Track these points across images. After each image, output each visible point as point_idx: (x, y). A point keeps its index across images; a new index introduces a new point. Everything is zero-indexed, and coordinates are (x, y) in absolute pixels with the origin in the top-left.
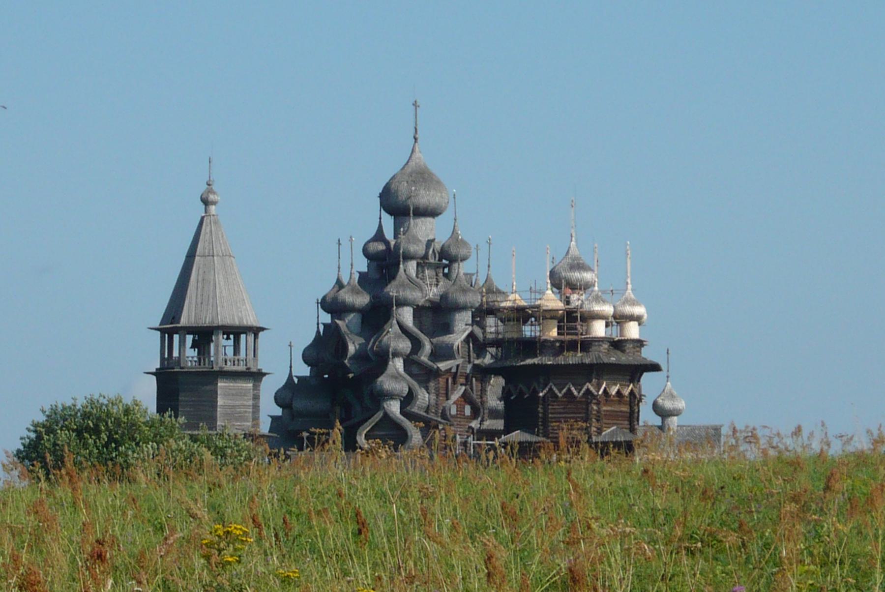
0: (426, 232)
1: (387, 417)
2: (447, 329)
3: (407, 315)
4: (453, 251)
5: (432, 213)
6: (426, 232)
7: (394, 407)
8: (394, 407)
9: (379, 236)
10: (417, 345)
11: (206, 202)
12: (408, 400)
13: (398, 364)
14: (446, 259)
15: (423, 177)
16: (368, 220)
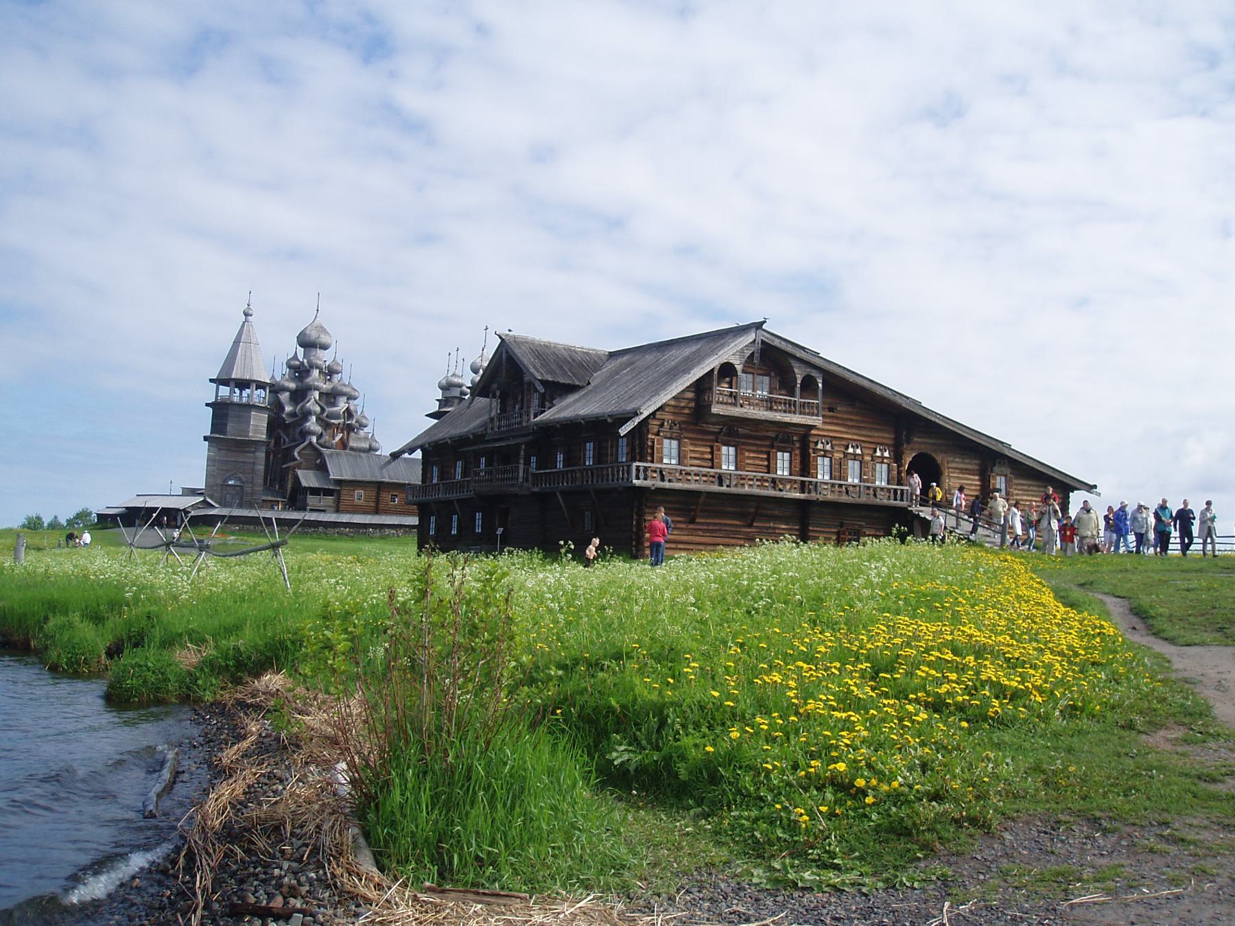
0: (324, 358)
1: (311, 443)
2: (334, 404)
3: (316, 394)
4: (335, 367)
5: (324, 347)
6: (324, 358)
7: (314, 439)
8: (314, 439)
9: (295, 357)
10: (323, 410)
11: (246, 314)
12: (320, 436)
13: (314, 418)
14: (330, 372)
15: (322, 329)
16: (291, 348)
